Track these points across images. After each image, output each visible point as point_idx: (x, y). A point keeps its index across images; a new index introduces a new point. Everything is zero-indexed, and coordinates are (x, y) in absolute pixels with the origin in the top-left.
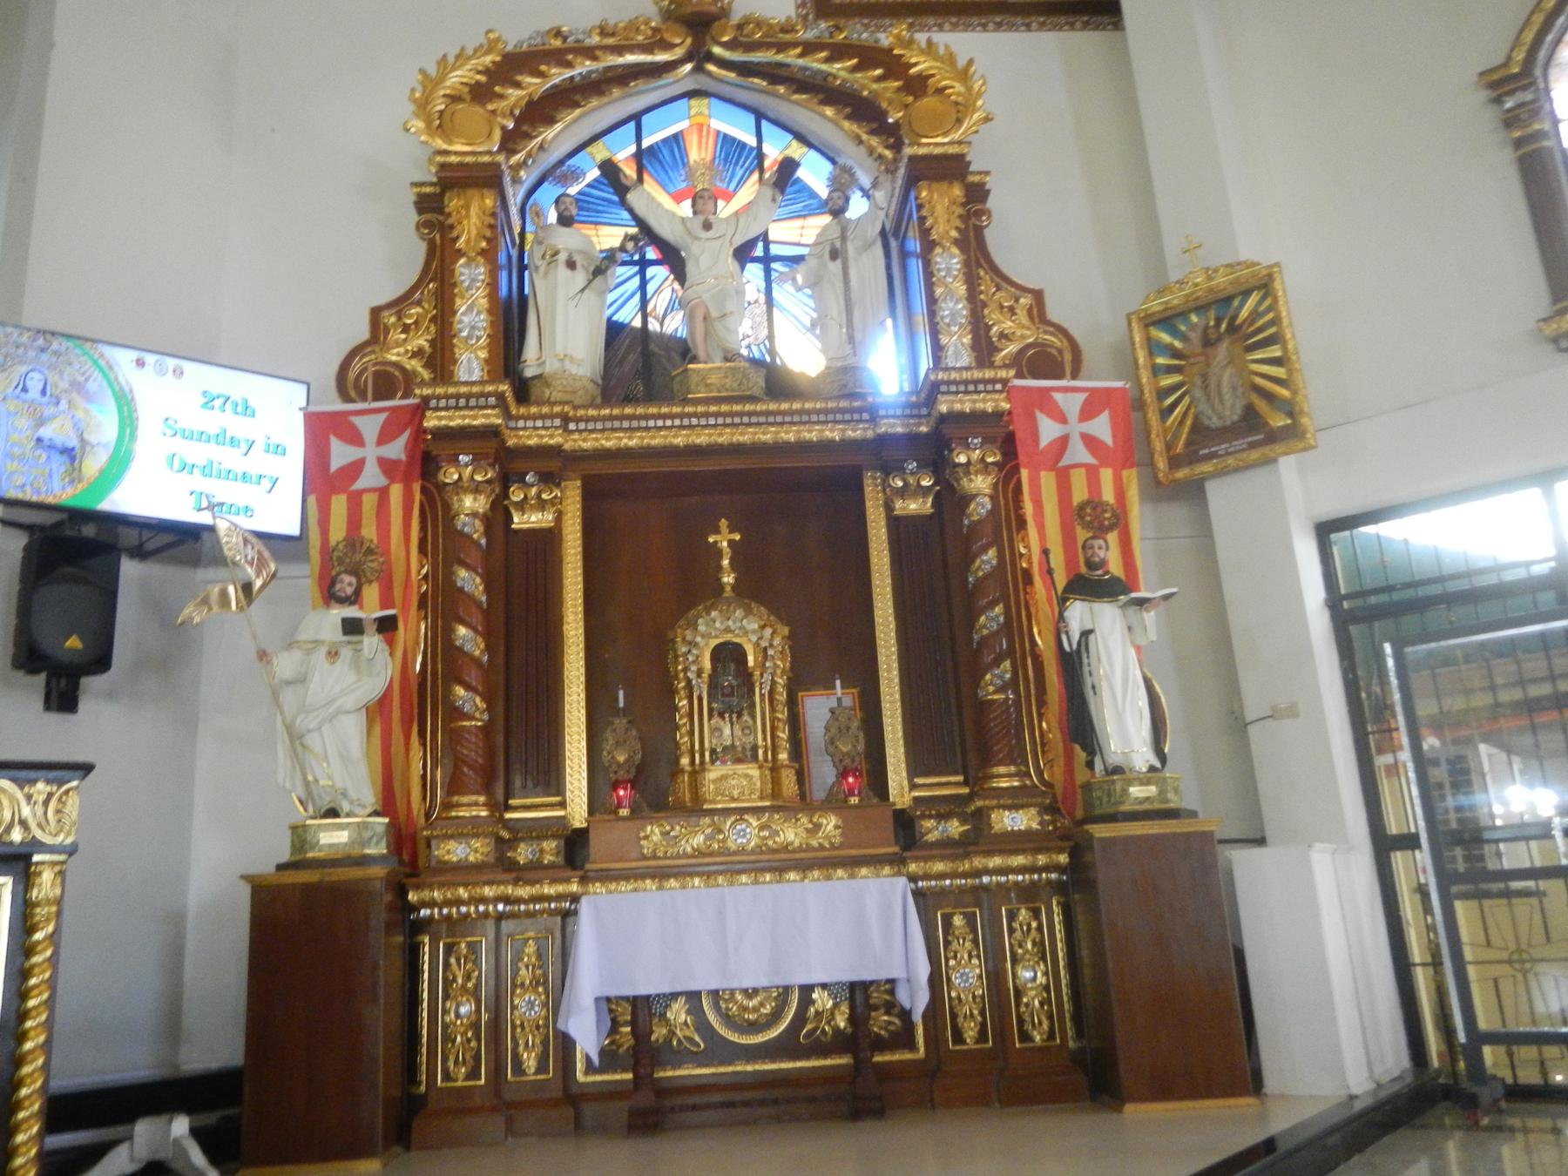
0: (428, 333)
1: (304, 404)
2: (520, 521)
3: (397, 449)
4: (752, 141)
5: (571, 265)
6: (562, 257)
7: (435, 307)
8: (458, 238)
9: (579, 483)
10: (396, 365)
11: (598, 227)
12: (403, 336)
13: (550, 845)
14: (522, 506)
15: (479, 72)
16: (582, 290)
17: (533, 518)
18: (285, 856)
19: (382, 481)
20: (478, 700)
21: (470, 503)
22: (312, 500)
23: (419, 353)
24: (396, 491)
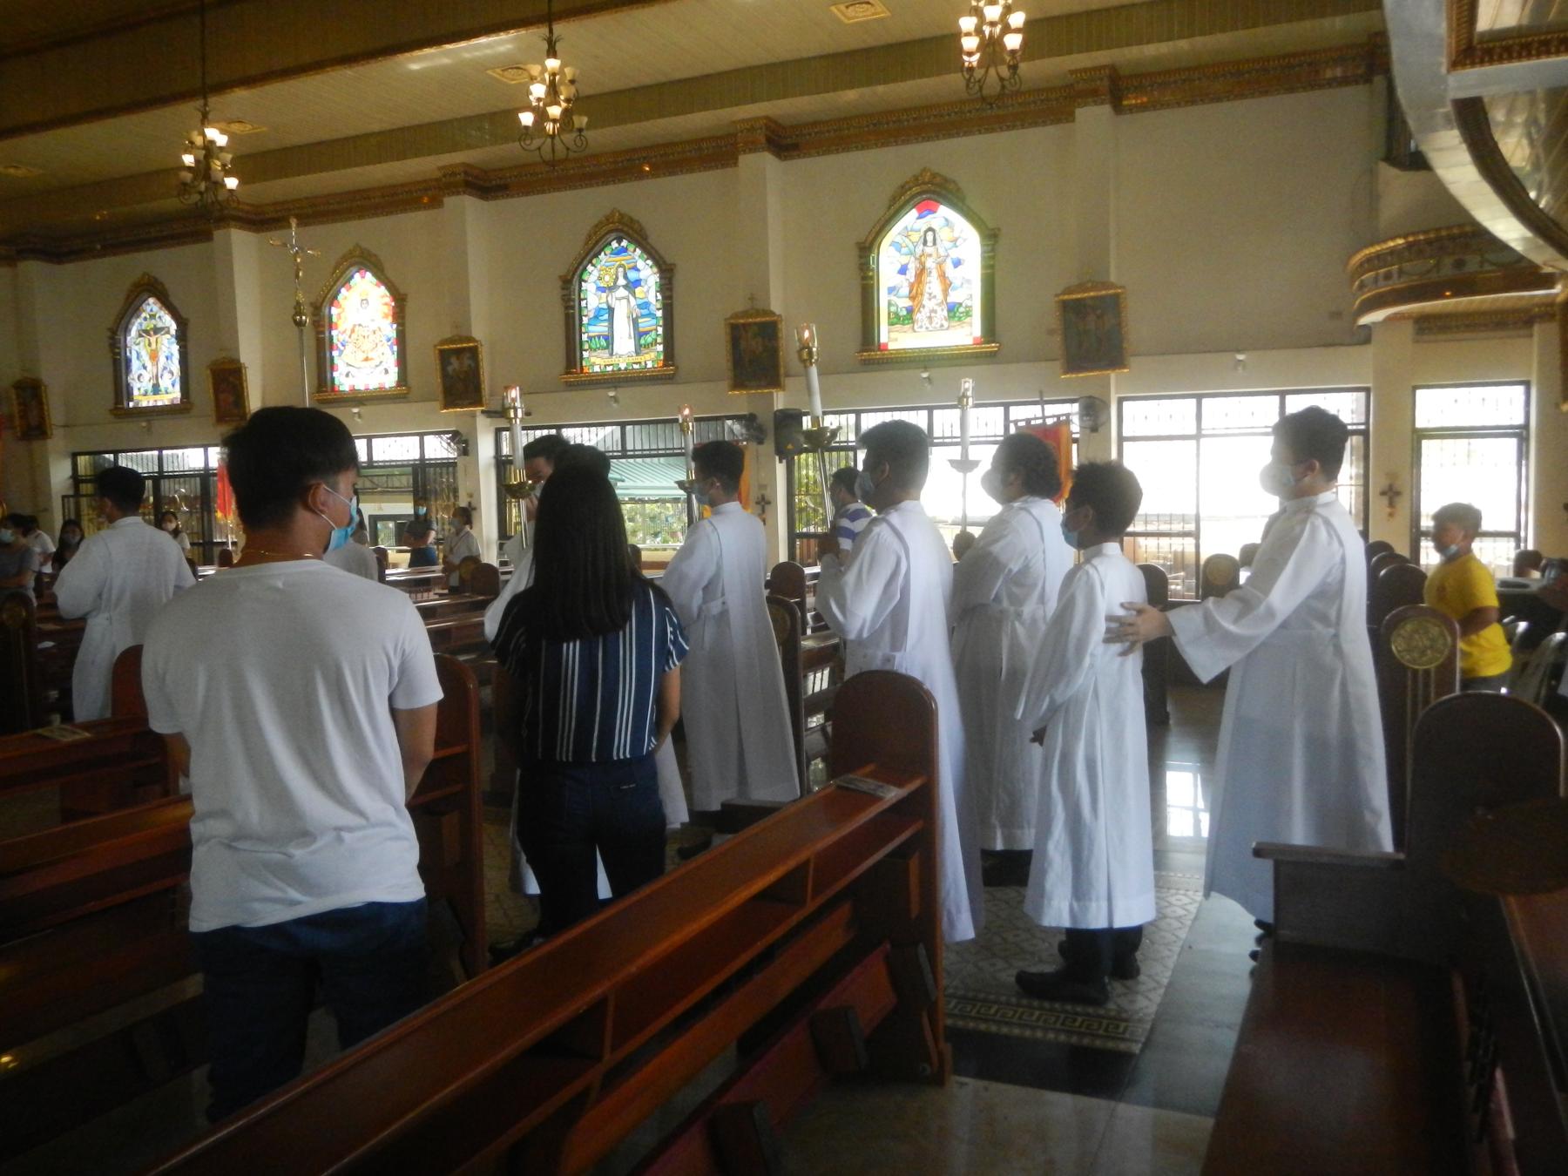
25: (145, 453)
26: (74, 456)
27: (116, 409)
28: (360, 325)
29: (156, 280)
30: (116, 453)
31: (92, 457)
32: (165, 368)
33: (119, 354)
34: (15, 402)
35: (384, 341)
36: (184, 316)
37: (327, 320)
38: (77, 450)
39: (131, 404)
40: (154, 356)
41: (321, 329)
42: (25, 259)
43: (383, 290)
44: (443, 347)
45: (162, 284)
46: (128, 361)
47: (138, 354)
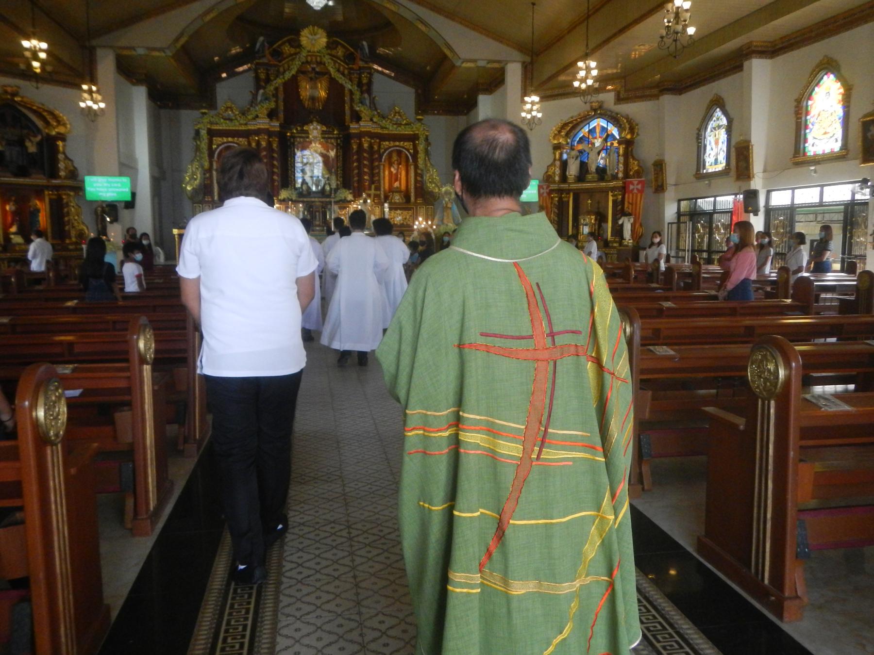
4: (606, 126)
5: (573, 158)
25: (706, 199)
26: (679, 201)
27: (696, 174)
28: (824, 110)
29: (720, 97)
30: (696, 199)
31: (688, 201)
32: (721, 149)
33: (701, 143)
34: (653, 173)
35: (837, 119)
36: (732, 117)
37: (804, 109)
38: (680, 198)
39: (705, 171)
40: (717, 143)
41: (799, 116)
42: (662, 95)
43: (839, 84)
44: (865, 120)
45: (723, 99)
46: (705, 146)
47: (710, 142)
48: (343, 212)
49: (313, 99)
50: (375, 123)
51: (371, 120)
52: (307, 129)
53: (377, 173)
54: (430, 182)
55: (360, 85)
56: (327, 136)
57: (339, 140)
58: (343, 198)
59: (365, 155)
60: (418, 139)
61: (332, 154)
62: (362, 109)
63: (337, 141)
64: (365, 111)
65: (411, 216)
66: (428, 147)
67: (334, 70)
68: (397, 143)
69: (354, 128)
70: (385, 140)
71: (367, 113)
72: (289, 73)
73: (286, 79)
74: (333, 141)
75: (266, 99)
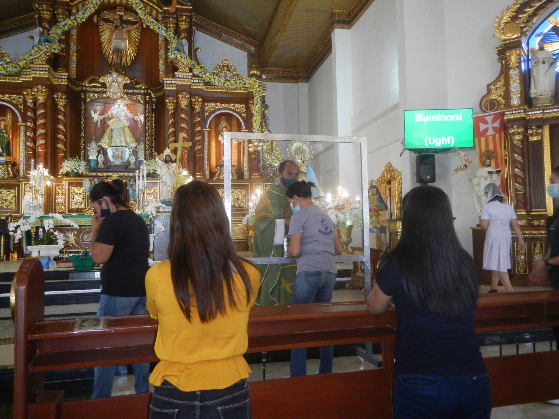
0: (503, 89)
1: (472, 115)
2: (531, 139)
3: (497, 124)
5: (544, 63)
6: (541, 60)
7: (504, 82)
8: (510, 64)
9: (548, 126)
10: (494, 100)
11: (552, 43)
12: (496, 91)
13: (543, 221)
14: (531, 135)
15: (513, 12)
16: (547, 71)
17: (535, 138)
18: (478, 223)
19: (493, 133)
20: (522, 187)
21: (517, 137)
22: (476, 139)
23: (500, 96)
24: (497, 135)
48: (152, 191)
49: (118, 51)
50: (194, 76)
51: (191, 70)
52: (103, 81)
53: (199, 140)
54: (268, 153)
55: (177, 32)
56: (131, 91)
57: (147, 97)
58: (152, 172)
59: (183, 116)
60: (253, 98)
61: (141, 118)
62: (179, 56)
63: (146, 98)
64: (182, 60)
65: (244, 196)
66: (265, 110)
67: (144, 13)
68: (225, 105)
69: (169, 84)
70: (209, 101)
71: (185, 62)
72: (84, 14)
73: (79, 21)
74: (139, 97)
75: (48, 41)
